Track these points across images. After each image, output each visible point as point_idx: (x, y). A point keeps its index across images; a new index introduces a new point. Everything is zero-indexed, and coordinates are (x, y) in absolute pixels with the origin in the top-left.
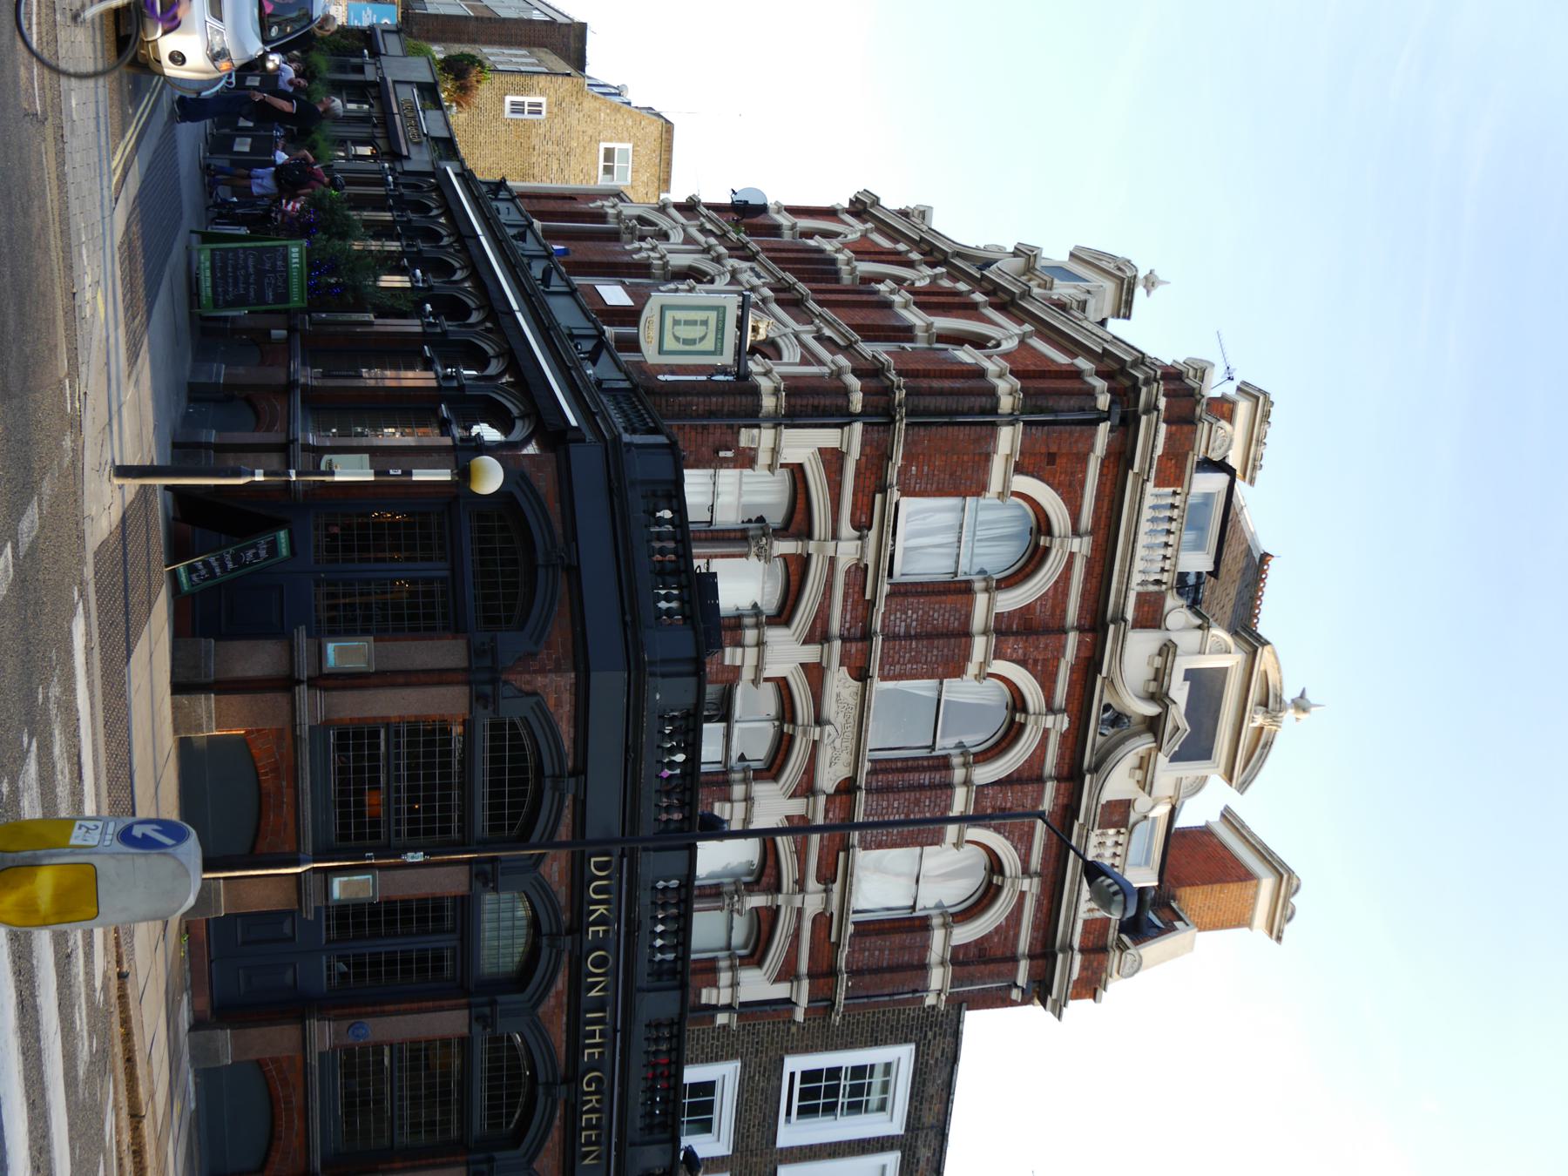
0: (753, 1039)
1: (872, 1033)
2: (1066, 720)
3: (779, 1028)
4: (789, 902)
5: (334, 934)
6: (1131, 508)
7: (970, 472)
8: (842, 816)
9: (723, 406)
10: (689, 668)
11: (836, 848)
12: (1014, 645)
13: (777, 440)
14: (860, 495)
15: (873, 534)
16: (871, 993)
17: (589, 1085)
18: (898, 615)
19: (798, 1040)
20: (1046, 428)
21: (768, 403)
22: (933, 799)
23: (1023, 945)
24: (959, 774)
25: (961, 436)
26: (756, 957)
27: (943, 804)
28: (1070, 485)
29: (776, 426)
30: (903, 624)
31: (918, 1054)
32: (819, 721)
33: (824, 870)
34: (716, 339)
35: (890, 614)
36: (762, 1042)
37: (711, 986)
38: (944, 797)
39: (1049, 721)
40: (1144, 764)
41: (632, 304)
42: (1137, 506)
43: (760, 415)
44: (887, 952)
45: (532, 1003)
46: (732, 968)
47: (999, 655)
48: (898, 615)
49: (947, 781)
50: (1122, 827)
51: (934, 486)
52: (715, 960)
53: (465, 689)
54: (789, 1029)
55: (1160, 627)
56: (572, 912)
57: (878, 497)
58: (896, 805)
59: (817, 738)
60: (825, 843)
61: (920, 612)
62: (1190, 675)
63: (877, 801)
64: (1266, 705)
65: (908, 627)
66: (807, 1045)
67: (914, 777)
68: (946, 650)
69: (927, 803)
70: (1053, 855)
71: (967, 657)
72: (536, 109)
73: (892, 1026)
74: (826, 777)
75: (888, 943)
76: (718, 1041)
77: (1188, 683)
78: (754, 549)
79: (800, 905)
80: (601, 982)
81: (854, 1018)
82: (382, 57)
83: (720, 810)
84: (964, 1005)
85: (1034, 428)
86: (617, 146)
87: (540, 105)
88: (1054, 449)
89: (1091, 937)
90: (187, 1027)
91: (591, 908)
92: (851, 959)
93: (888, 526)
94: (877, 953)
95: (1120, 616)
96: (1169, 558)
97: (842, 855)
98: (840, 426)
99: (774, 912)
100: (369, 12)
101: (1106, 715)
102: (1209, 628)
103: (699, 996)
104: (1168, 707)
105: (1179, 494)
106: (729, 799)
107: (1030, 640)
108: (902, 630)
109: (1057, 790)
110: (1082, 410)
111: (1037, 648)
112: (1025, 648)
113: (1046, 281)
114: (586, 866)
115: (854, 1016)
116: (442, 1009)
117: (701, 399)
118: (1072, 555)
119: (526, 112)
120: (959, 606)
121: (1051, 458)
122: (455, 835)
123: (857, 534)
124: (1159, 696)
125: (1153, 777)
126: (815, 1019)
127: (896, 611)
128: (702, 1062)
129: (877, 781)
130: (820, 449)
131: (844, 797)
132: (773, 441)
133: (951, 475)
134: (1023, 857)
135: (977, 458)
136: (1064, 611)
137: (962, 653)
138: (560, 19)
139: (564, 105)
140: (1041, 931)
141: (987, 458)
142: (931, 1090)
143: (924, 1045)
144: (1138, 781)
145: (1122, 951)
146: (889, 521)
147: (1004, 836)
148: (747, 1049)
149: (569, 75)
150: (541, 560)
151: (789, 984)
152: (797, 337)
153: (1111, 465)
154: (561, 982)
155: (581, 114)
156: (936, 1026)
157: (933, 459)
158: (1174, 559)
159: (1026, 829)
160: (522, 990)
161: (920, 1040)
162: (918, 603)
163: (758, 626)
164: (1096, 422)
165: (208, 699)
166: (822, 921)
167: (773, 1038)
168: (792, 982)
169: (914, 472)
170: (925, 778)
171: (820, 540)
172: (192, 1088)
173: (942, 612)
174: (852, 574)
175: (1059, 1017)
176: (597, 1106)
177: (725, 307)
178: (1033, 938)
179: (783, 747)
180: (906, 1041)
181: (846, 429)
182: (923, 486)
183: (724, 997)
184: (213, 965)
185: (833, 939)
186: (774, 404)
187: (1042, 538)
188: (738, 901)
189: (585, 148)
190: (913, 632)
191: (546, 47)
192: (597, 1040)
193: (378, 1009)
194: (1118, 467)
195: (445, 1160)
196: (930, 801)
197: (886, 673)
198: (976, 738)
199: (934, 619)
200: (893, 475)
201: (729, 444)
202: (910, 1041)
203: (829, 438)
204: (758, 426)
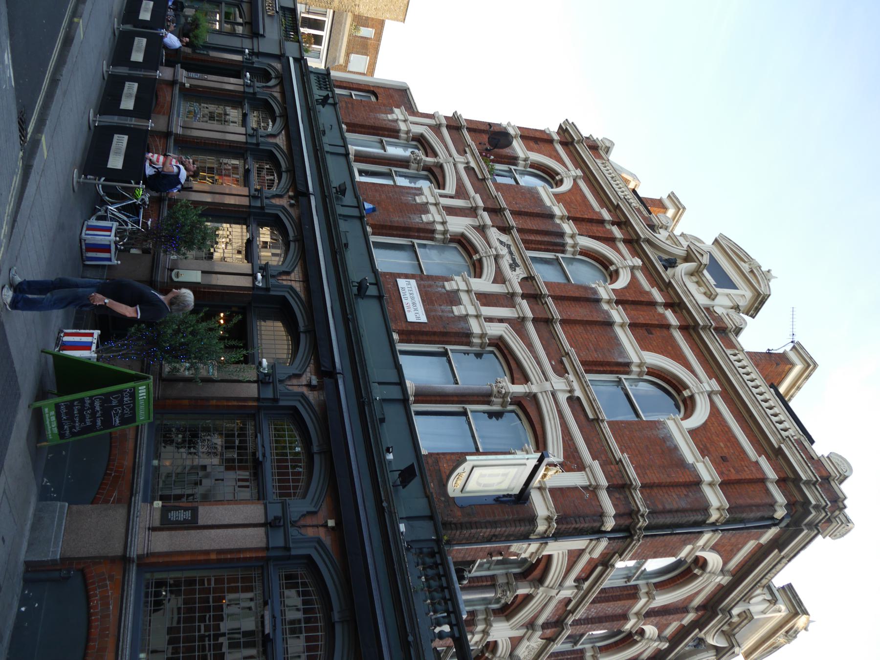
21: (541, 527)
41: (423, 319)
95: (728, 609)
113: (712, 294)
171: (547, 587)
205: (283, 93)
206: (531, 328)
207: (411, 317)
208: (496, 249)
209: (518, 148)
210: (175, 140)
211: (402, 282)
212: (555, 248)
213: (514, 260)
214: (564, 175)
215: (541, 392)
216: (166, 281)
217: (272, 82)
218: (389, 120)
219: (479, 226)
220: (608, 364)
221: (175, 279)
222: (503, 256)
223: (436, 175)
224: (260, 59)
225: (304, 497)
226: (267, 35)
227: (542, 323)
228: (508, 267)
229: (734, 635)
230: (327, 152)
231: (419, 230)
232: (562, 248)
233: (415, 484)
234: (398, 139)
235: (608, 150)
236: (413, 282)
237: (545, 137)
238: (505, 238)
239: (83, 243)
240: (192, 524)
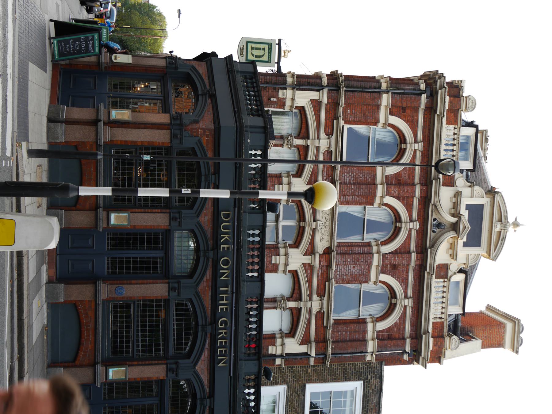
0: (292, 374)
1: (344, 375)
2: (418, 224)
3: (303, 369)
4: (305, 305)
5: (110, 247)
6: (438, 130)
7: (371, 114)
8: (326, 264)
9: (272, 80)
10: (262, 130)
11: (324, 281)
12: (394, 190)
13: (294, 95)
14: (328, 121)
15: (334, 137)
16: (343, 352)
17: (221, 325)
18: (346, 174)
19: (311, 376)
20: (401, 95)
22: (364, 259)
23: (407, 333)
24: (375, 249)
25: (367, 97)
26: (292, 333)
27: (369, 261)
28: (412, 122)
29: (293, 89)
30: (348, 178)
31: (365, 387)
32: (315, 220)
33: (320, 291)
34: (268, 56)
35: (342, 174)
36: (296, 376)
37: (273, 346)
38: (369, 258)
39: (411, 225)
40: (453, 247)
42: (440, 129)
43: (287, 85)
44: (348, 333)
45: (196, 283)
46: (282, 337)
47: (388, 194)
48: (346, 174)
49: (370, 252)
50: (445, 278)
51: (357, 119)
52: (274, 334)
53: (169, 131)
54: (307, 370)
55: (454, 186)
56: (213, 240)
57: (335, 121)
58: (349, 261)
59: (314, 227)
60: (320, 278)
61: (355, 174)
62: (468, 207)
63: (341, 258)
64: (501, 221)
65: (350, 180)
66: (315, 379)
67: (356, 249)
68: (366, 190)
69: (362, 261)
70: (417, 290)
71: (375, 194)
73: (353, 371)
74: (319, 246)
75: (348, 329)
76: (276, 374)
77: (468, 211)
78: (286, 142)
79: (310, 307)
80: (227, 272)
81: (335, 367)
83: (275, 260)
84: (384, 362)
85: (396, 95)
88: (404, 105)
89: (436, 331)
90: (45, 282)
91: (222, 236)
92: (333, 335)
93: (340, 133)
94: (344, 333)
96: (455, 156)
97: (327, 283)
98: (318, 90)
99: (299, 310)
101: (435, 222)
102: (474, 186)
103: (268, 350)
104: (460, 217)
105: (456, 128)
106: (278, 255)
107: (401, 188)
108: (348, 181)
109: (417, 257)
110: (414, 90)
111: (404, 191)
112: (399, 191)
114: (217, 310)
115: (336, 365)
116: (157, 283)
117: (263, 77)
118: (415, 151)
120: (370, 172)
121: (404, 109)
122: (161, 353)
123: (327, 137)
124: (456, 214)
125: (457, 251)
126: (318, 366)
127: (345, 172)
128: (270, 385)
129: (341, 250)
130: (311, 100)
131: (327, 255)
132: (292, 95)
133: (364, 114)
134: (404, 290)
135: (374, 108)
136: (414, 176)
137: (373, 192)
140: (415, 327)
141: (378, 107)
142: (371, 406)
143: (367, 382)
144: (450, 255)
145: (450, 337)
146: (340, 131)
147: (396, 279)
148: (289, 379)
150: (200, 93)
151: (307, 346)
153: (428, 114)
154: (208, 275)
156: (372, 372)
157: (356, 107)
158: (457, 156)
159: (405, 277)
160: (192, 278)
161: (365, 379)
162: (354, 169)
163: (288, 176)
164: (421, 94)
165: (62, 126)
166: (320, 315)
167: (300, 374)
168: (308, 345)
169: (349, 112)
170: (361, 250)
172: (46, 314)
173: (363, 174)
174: (326, 155)
175: (425, 368)
176: (225, 335)
177: (271, 43)
178: (411, 330)
179: (300, 233)
180: (359, 379)
181: (321, 91)
182: (353, 118)
183: (279, 352)
184: (58, 256)
185: (325, 325)
186: (292, 81)
187: (403, 145)
188: (284, 303)
190: (352, 183)
192: (225, 302)
193: (129, 281)
194: (431, 115)
195: (156, 362)
196: (363, 260)
197: (342, 200)
198: (380, 236)
199: (360, 177)
200: (341, 111)
201: (275, 96)
202: (361, 380)
203: (314, 95)
204: (286, 89)
221: (115, 61)
229: (459, 213)
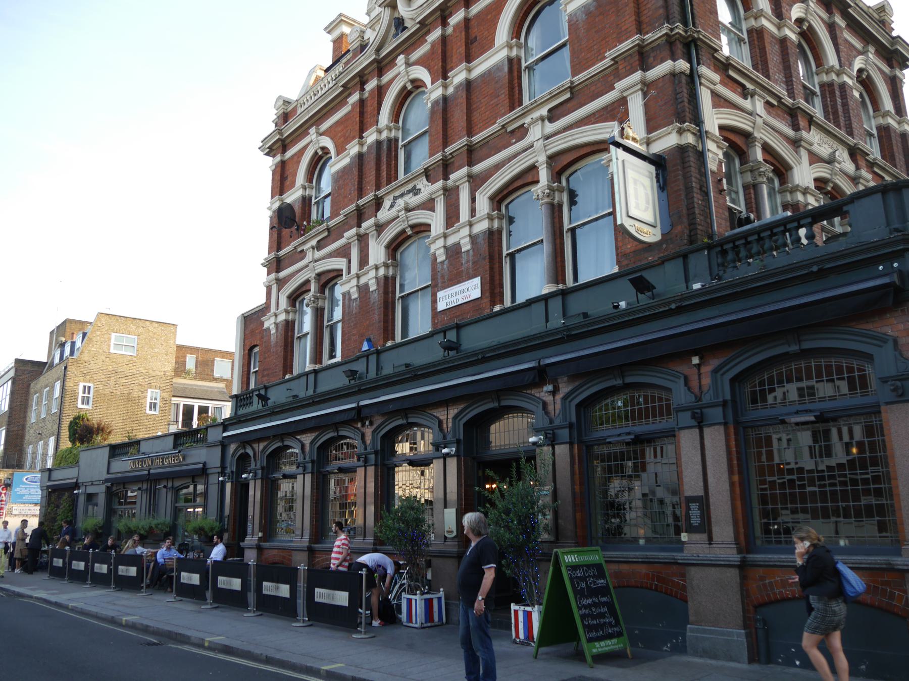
21: (690, 139)
41: (477, 281)
72: (87, 389)
82: (80, 481)
86: (113, 341)
87: (85, 387)
100: (18, 489)
119: (88, 396)
138: (12, 374)
139: (85, 372)
149: (66, 368)
152: (547, 138)
155: (92, 362)
171: (753, 128)
189: (113, 362)
191: (30, 384)
205: (259, 440)
206: (478, 168)
207: (476, 294)
208: (399, 211)
209: (293, 196)
210: (316, 543)
211: (441, 306)
212: (393, 149)
213: (409, 192)
214: (316, 147)
215: (546, 151)
216: (457, 543)
217: (250, 451)
218: (277, 331)
219: (377, 230)
220: (511, 82)
221: (455, 534)
222: (406, 203)
223: (328, 280)
224: (228, 465)
225: (669, 390)
226: (203, 460)
227: (473, 156)
228: (417, 197)
230: (314, 392)
231: (386, 292)
232: (393, 142)
233: (649, 276)
234: (295, 321)
235: (287, 102)
236: (440, 294)
237: (279, 169)
238: (387, 203)
239: (425, 625)
240: (704, 501)
